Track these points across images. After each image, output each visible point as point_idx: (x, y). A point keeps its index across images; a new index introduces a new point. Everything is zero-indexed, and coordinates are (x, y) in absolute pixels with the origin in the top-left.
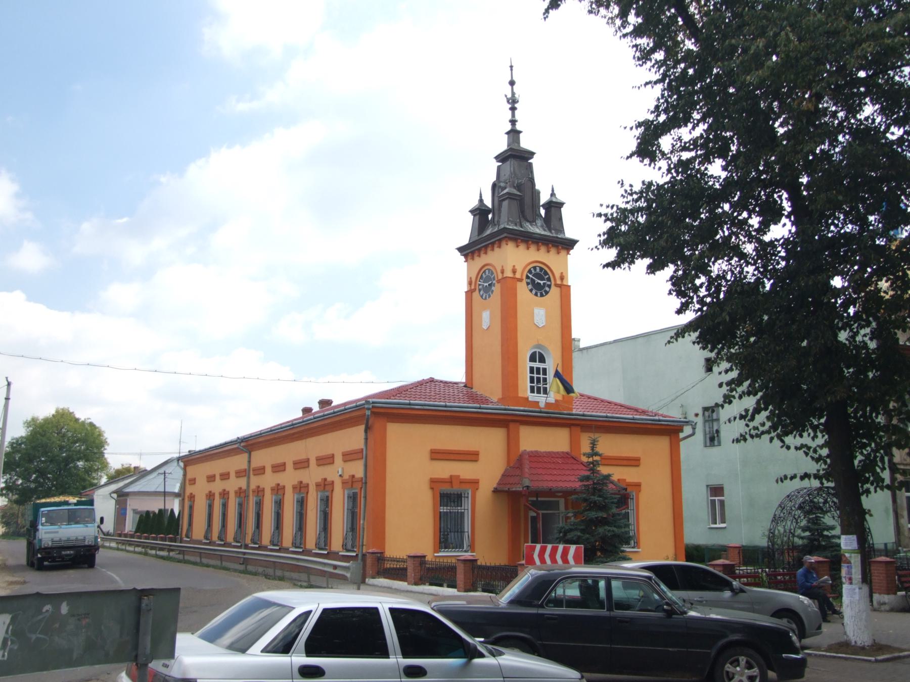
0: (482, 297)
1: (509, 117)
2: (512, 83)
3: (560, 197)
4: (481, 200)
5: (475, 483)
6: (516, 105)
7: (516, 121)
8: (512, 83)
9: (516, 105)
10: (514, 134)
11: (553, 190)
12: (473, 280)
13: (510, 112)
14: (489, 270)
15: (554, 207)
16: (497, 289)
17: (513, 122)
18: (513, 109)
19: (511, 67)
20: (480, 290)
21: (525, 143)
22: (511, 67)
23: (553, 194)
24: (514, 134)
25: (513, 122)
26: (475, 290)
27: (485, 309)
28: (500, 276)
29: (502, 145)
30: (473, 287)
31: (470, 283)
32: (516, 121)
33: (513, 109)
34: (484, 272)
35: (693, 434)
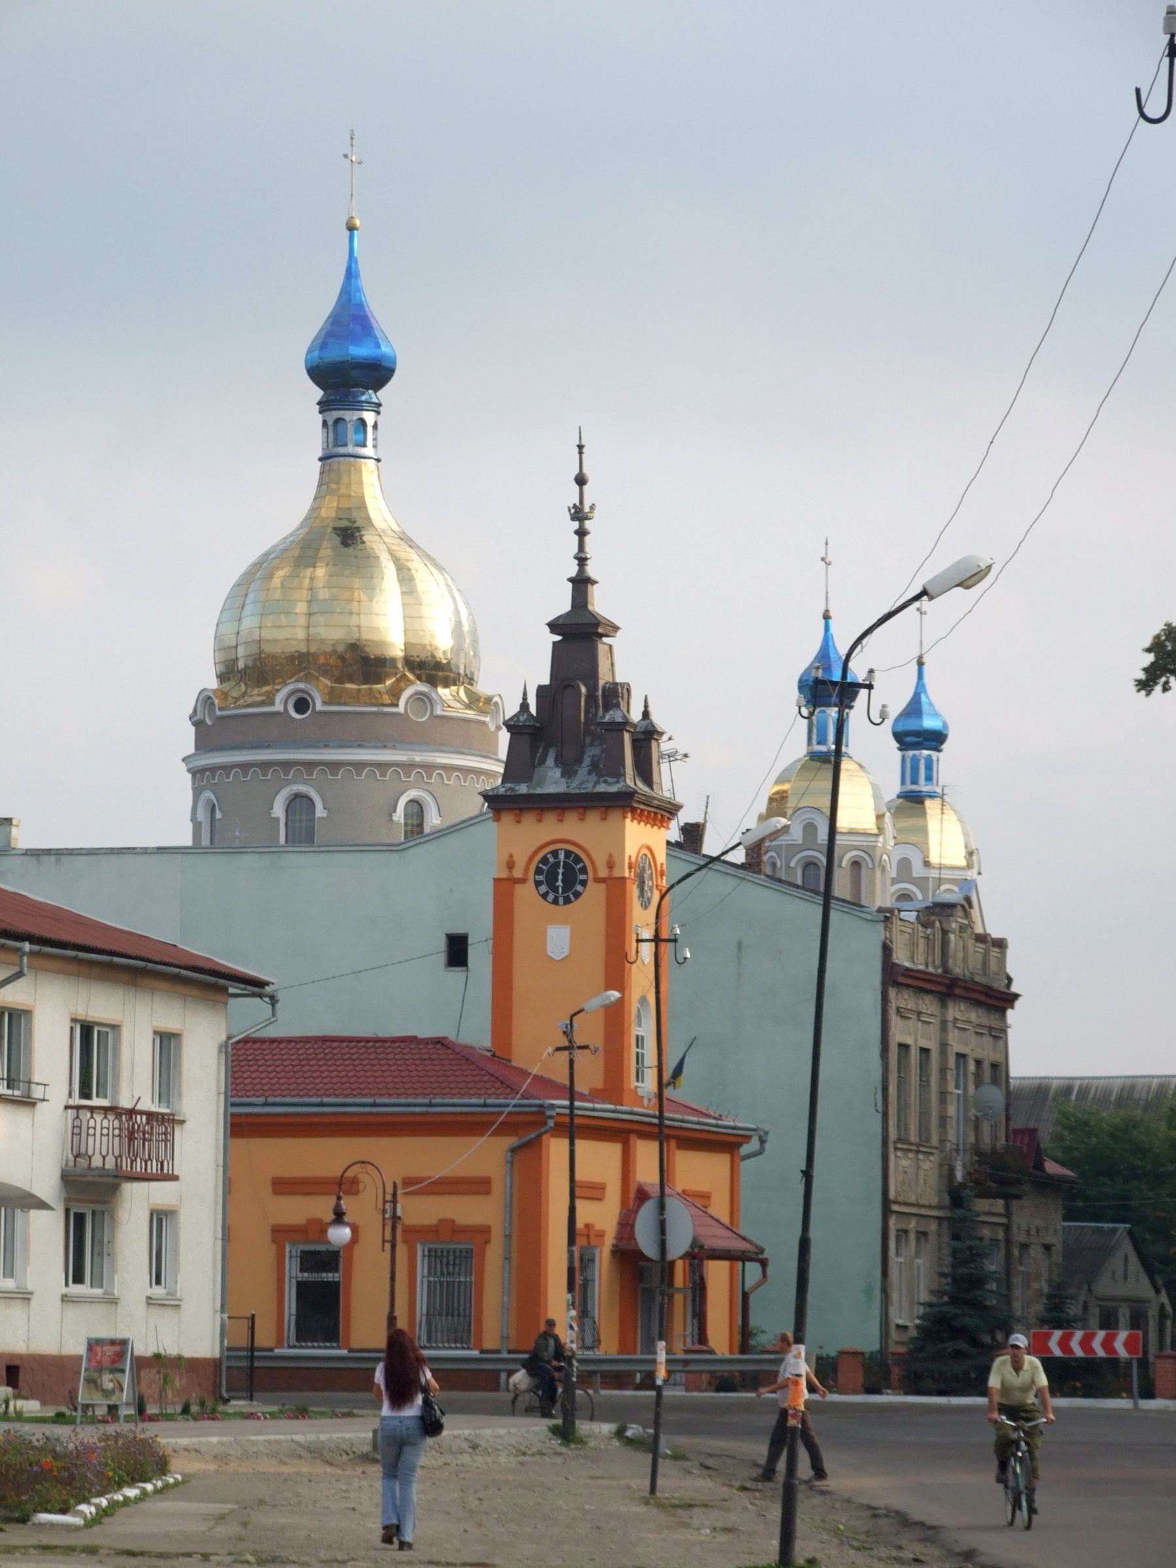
0: (544, 896)
1: (576, 550)
2: (581, 481)
3: (657, 719)
4: (524, 706)
5: (483, 1232)
6: (588, 524)
7: (586, 559)
8: (581, 481)
9: (588, 524)
10: (581, 584)
11: (646, 706)
12: (521, 861)
13: (576, 538)
14: (568, 853)
15: (647, 736)
16: (593, 896)
17: (582, 561)
18: (581, 533)
19: (581, 447)
20: (538, 884)
21: (601, 603)
22: (581, 447)
23: (646, 714)
24: (581, 584)
25: (582, 561)
26: (523, 881)
27: (552, 922)
28: (603, 873)
29: (562, 604)
30: (518, 873)
31: (511, 865)
32: (586, 559)
33: (581, 533)
34: (555, 853)
35: (760, 1152)
